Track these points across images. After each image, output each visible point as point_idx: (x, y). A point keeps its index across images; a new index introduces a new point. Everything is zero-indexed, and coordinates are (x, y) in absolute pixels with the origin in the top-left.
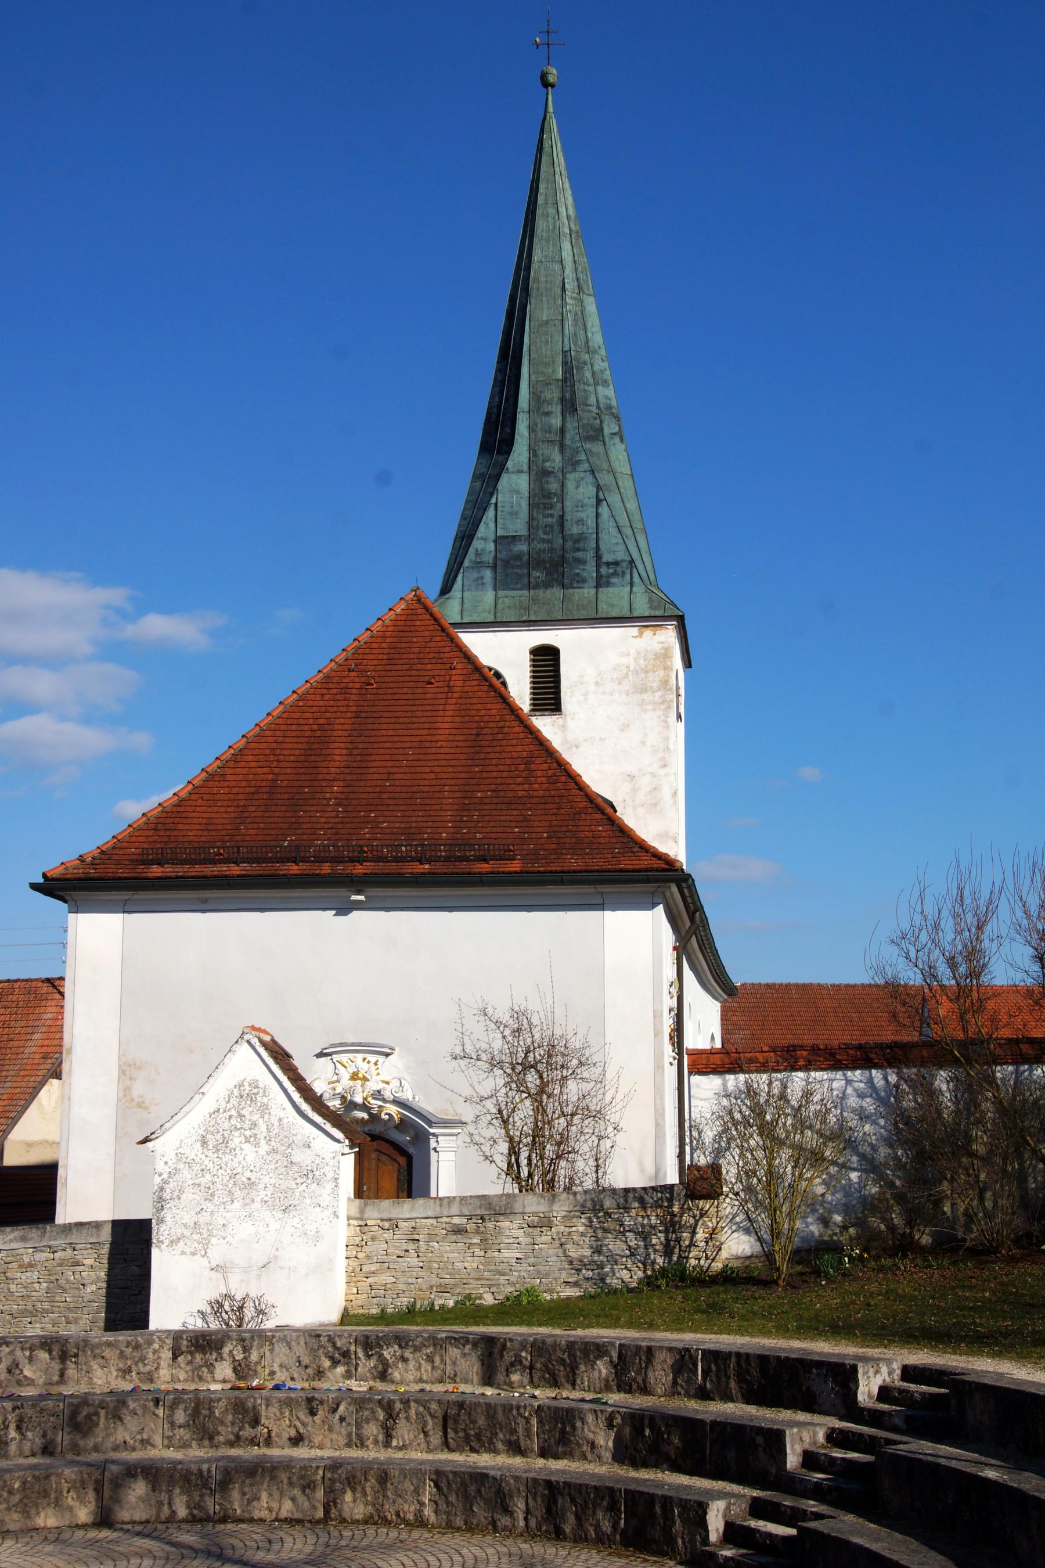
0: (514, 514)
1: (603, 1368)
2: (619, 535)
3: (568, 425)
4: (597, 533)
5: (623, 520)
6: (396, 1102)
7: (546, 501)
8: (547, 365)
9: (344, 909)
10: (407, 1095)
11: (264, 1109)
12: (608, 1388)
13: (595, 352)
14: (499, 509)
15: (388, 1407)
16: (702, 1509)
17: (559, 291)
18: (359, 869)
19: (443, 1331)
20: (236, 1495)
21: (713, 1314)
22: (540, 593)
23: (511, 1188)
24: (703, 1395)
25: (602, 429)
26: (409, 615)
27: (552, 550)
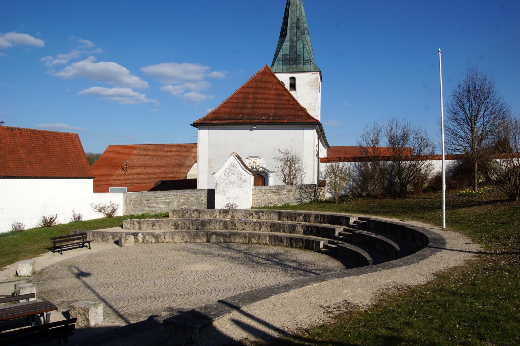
0: (287, 50)
1: (301, 218)
5: (309, 51)
6: (262, 168)
9: (252, 129)
10: (264, 166)
11: (236, 168)
12: (302, 221)
15: (260, 224)
16: (319, 242)
18: (255, 121)
19: (271, 210)
20: (232, 238)
21: (323, 208)
23: (284, 184)
24: (320, 222)
26: (265, 70)
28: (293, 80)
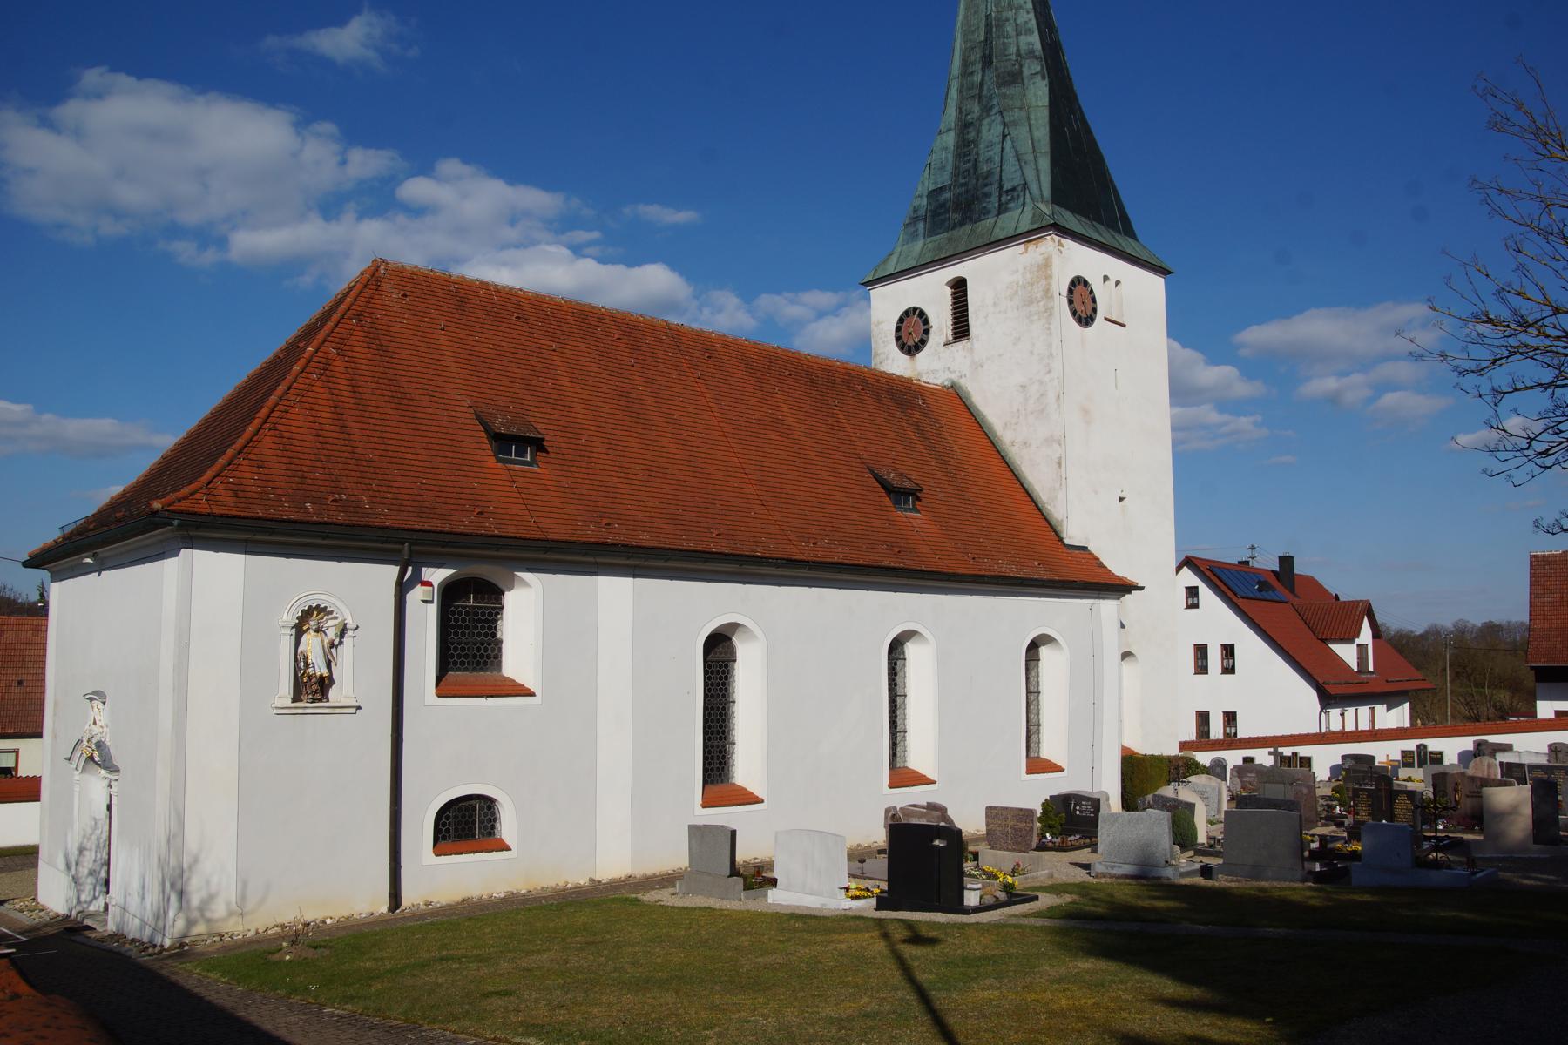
13: (1021, 7)
22: (955, 232)
28: (959, 286)
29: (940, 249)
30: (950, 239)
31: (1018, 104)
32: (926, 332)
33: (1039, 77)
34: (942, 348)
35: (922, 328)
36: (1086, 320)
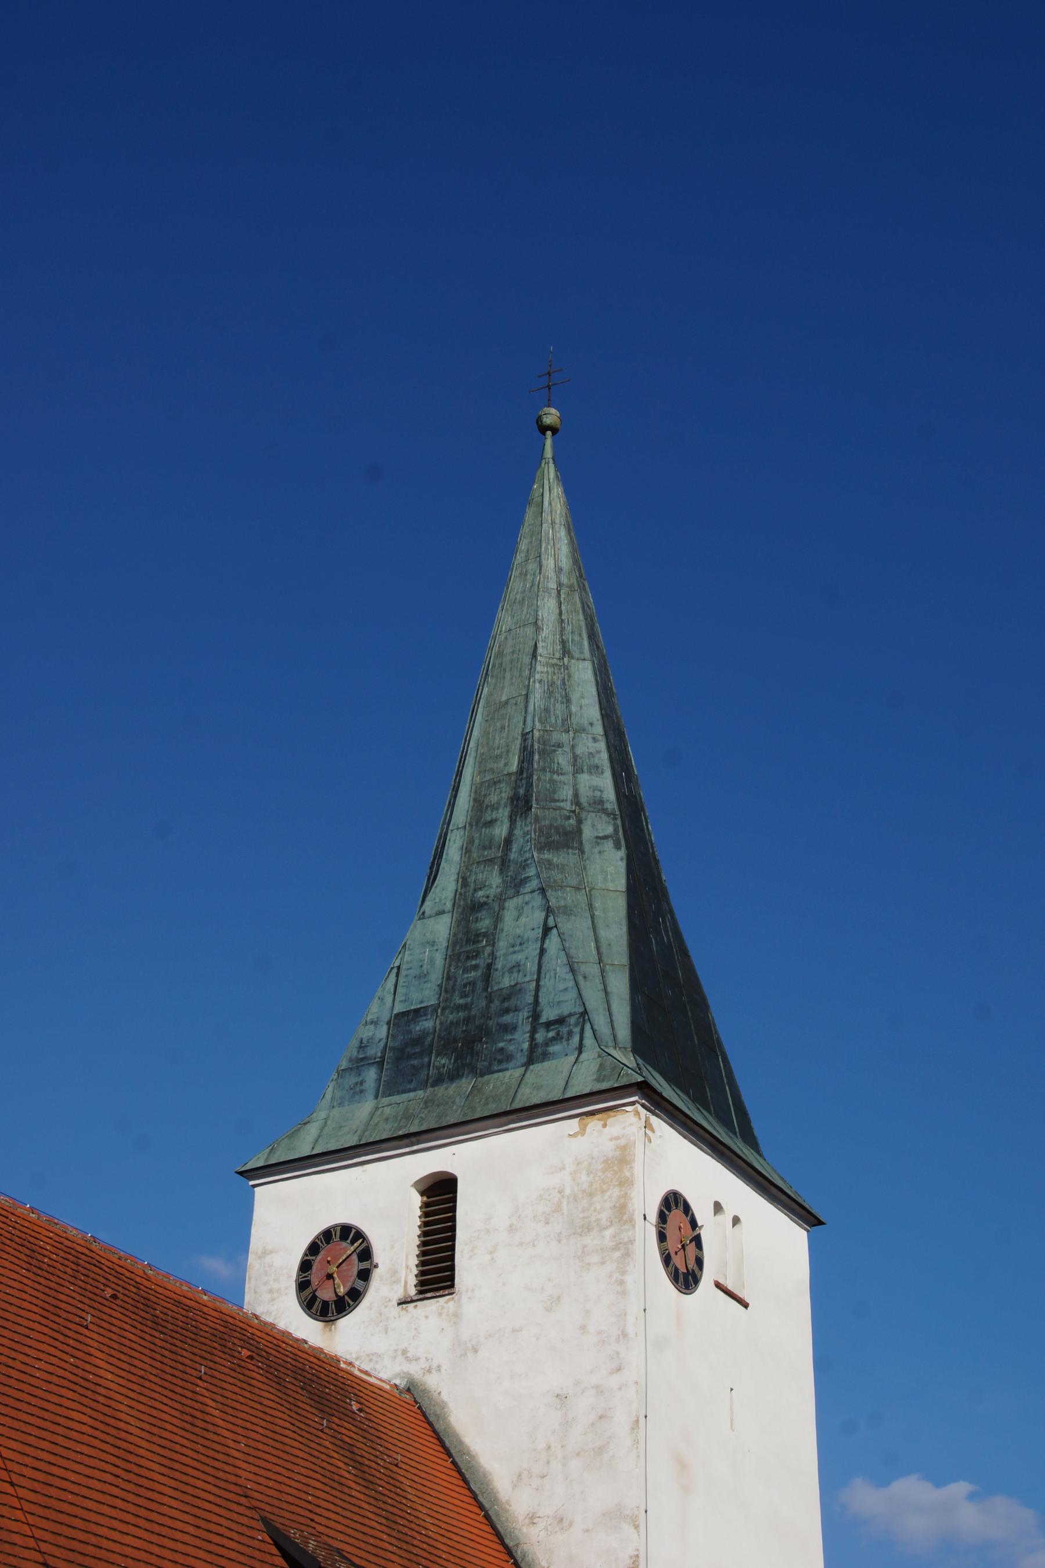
2: (570, 976)
3: (517, 832)
4: (538, 980)
7: (470, 948)
8: (498, 757)
13: (584, 730)
14: (403, 973)
17: (527, 659)
22: (441, 1091)
25: (580, 832)
27: (468, 1020)
28: (440, 1192)
29: (408, 1117)
30: (427, 1103)
31: (573, 881)
32: (365, 1275)
33: (609, 845)
34: (395, 1310)
35: (356, 1266)
36: (686, 1279)
